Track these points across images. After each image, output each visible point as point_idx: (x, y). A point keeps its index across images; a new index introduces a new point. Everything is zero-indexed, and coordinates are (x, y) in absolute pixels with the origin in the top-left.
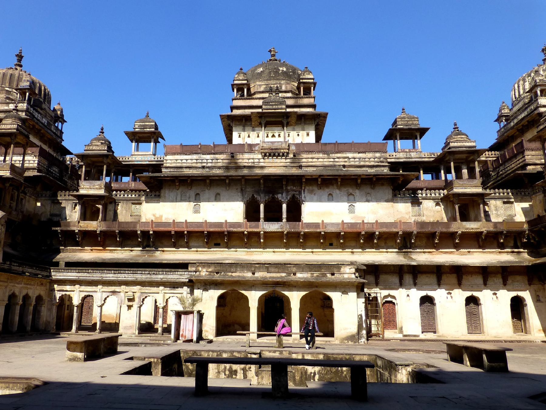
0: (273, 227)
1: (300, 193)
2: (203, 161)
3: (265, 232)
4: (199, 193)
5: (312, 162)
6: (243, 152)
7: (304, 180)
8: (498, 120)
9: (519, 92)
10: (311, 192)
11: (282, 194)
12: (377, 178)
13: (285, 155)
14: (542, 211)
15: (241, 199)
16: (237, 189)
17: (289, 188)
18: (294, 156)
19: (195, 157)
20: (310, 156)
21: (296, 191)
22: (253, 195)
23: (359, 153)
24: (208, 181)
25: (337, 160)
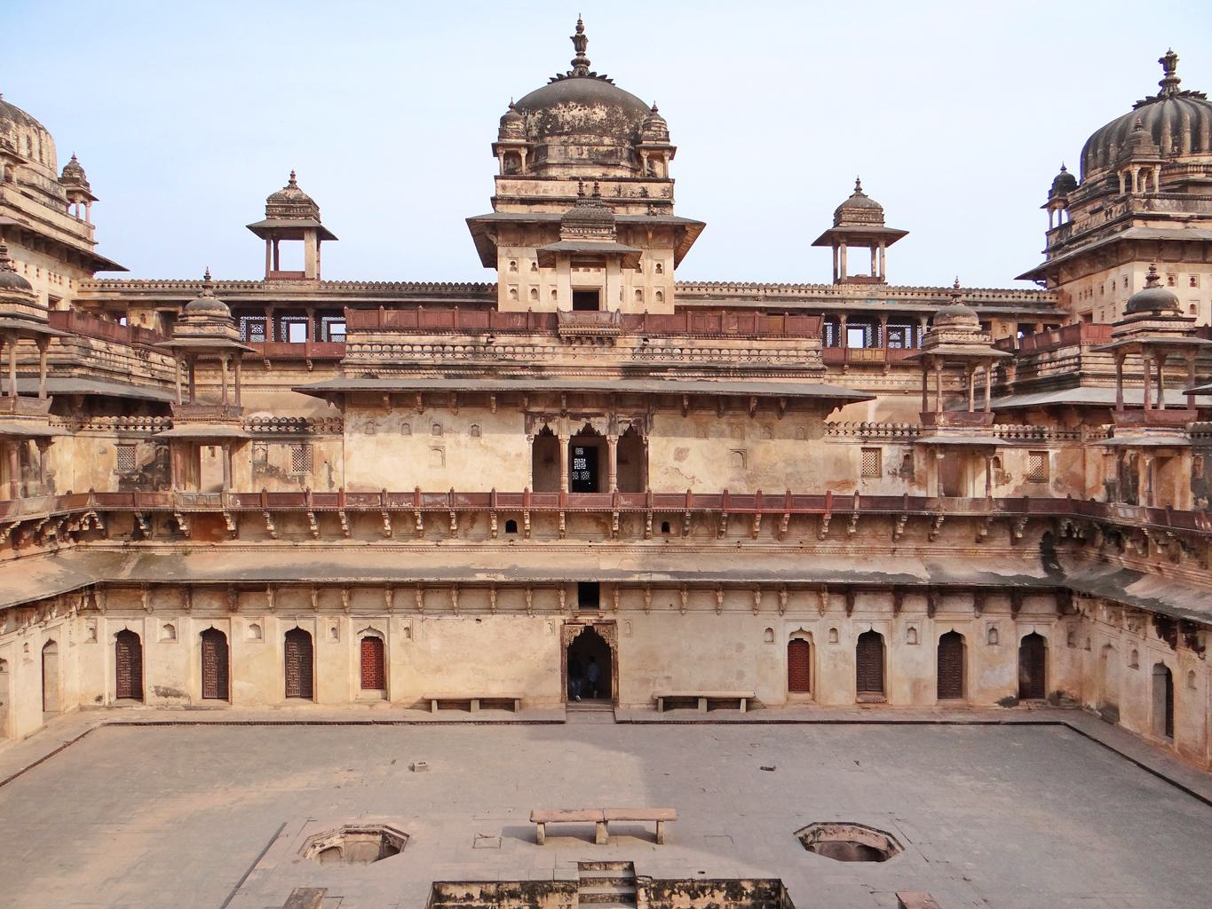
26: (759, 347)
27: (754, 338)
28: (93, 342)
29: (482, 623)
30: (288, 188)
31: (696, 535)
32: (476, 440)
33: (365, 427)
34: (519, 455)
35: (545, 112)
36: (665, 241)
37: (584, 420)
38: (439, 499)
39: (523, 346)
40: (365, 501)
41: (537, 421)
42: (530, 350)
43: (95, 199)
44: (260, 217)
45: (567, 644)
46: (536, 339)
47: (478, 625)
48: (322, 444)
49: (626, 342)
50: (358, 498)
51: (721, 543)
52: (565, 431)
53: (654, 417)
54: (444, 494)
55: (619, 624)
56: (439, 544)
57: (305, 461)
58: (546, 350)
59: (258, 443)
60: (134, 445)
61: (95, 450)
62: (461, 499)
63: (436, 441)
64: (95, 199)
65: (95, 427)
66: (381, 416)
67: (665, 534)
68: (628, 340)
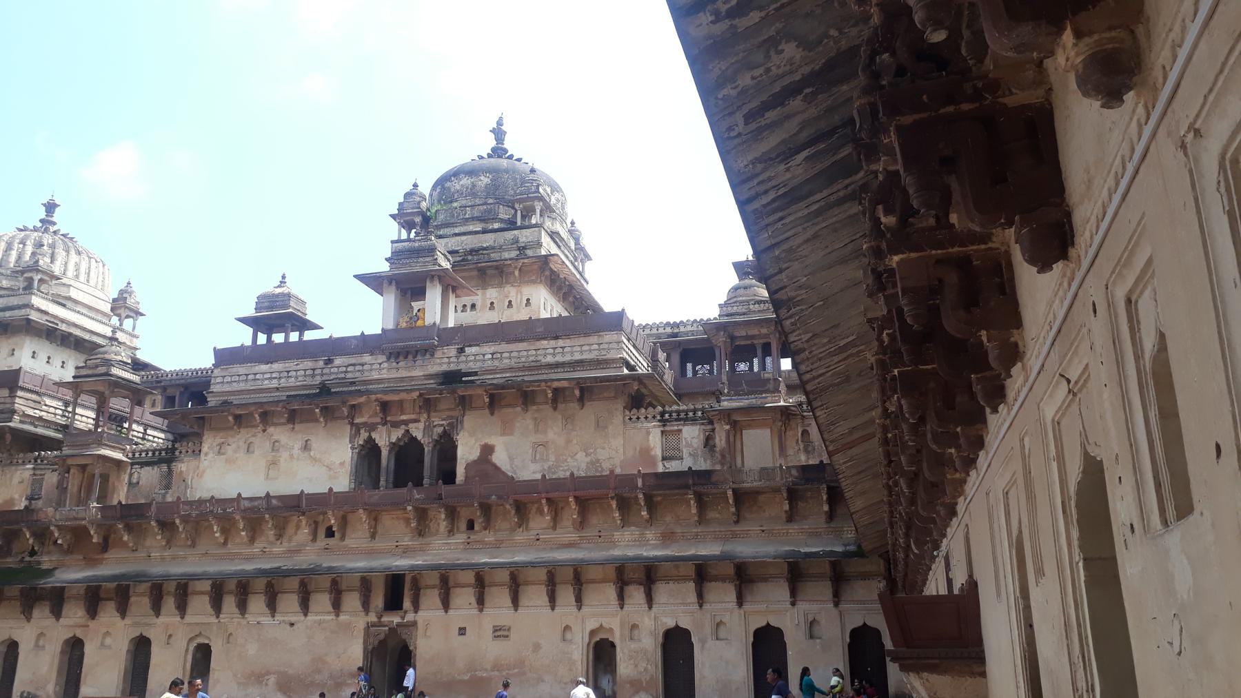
14: (21, 497)
26: (563, 345)
27: (556, 338)
28: (48, 401)
29: (295, 627)
31: (499, 530)
32: (306, 454)
33: (218, 447)
34: (342, 464)
35: (443, 187)
37: (403, 426)
38: (256, 503)
39: (354, 365)
40: (197, 509)
41: (362, 431)
42: (358, 368)
43: (142, 315)
44: (250, 311)
45: (370, 647)
46: (367, 358)
50: (192, 505)
52: (384, 439)
53: (465, 418)
54: (261, 498)
56: (265, 550)
57: (167, 481)
59: (135, 466)
60: (44, 474)
61: (16, 480)
62: (274, 502)
63: (273, 456)
64: (142, 315)
65: (20, 461)
66: (233, 436)
67: (469, 531)
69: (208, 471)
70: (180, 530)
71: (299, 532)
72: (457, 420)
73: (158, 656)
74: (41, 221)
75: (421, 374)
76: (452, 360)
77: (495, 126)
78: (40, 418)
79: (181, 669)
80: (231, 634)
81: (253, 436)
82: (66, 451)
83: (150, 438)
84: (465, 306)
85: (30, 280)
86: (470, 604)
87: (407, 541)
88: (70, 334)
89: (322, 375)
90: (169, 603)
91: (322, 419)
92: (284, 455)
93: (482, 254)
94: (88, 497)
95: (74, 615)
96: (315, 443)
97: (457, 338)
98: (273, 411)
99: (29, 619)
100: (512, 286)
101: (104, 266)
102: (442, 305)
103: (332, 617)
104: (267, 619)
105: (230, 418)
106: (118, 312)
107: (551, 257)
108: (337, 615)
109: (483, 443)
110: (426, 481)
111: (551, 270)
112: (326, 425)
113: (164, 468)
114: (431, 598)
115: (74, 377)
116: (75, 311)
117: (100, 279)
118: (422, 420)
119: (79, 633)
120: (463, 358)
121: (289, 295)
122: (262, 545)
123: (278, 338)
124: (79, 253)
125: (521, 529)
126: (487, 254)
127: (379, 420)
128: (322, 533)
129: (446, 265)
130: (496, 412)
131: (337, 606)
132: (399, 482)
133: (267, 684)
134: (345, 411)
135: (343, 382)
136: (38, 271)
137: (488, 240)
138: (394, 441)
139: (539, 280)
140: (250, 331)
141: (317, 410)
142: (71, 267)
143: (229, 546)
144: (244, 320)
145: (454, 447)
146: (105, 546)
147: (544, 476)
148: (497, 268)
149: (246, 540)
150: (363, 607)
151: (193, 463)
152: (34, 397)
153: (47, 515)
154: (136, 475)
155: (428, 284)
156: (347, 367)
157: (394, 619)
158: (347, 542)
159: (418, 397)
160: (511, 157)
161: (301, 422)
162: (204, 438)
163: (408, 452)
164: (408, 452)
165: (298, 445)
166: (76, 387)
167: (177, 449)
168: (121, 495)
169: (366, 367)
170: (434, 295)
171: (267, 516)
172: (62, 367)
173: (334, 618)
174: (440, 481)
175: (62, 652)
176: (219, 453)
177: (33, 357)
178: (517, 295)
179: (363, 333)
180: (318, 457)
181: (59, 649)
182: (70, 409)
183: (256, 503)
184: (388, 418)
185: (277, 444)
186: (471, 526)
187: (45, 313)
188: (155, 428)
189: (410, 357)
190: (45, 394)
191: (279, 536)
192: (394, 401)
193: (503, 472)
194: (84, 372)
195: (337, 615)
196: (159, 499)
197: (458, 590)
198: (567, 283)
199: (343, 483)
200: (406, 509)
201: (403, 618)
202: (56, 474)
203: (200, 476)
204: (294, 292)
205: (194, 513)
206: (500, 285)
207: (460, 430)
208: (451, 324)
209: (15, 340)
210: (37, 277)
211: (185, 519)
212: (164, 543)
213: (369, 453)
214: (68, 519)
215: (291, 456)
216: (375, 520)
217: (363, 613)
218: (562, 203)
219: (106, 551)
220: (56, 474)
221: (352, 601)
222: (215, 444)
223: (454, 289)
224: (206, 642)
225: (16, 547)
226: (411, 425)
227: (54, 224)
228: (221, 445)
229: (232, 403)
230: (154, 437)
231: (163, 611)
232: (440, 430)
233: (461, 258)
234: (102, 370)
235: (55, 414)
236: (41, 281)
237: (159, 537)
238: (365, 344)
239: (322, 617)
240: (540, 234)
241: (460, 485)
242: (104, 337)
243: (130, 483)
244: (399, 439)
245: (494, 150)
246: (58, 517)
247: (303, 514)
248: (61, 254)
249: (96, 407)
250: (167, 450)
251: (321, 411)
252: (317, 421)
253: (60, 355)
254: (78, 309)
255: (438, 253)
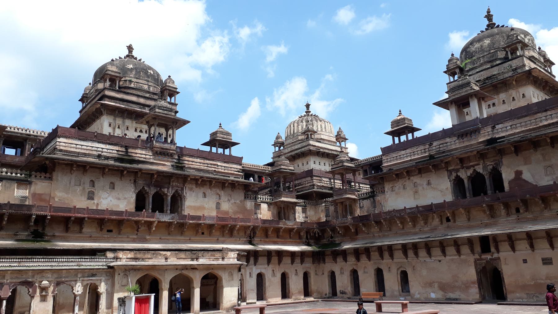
0: (166, 218)
1: (182, 189)
2: (99, 149)
3: (159, 222)
4: (94, 180)
5: (192, 165)
6: (136, 148)
7: (189, 179)
8: (275, 145)
9: (294, 129)
10: (191, 189)
11: (168, 189)
12: (238, 184)
13: (171, 155)
15: (134, 189)
16: (130, 180)
17: (174, 184)
18: (179, 157)
19: (90, 144)
20: (191, 159)
21: (179, 187)
22: (143, 186)
23: (225, 162)
24: (107, 170)
25: (209, 166)
26: (550, 114)
27: (546, 111)
28: (324, 179)
30: (399, 116)
32: (430, 186)
34: (447, 189)
35: (466, 52)
36: (524, 82)
37: (472, 168)
38: (413, 210)
39: (443, 144)
41: (453, 173)
42: (445, 145)
43: (347, 139)
44: (389, 129)
45: (479, 270)
46: (448, 140)
47: (441, 262)
48: (379, 197)
49: (485, 130)
51: (547, 214)
52: (464, 175)
53: (503, 159)
55: (501, 259)
58: (452, 143)
62: (421, 209)
63: (415, 189)
64: (347, 139)
65: (320, 203)
66: (397, 183)
68: (486, 129)
69: (389, 199)
70: (384, 224)
71: (434, 221)
72: (499, 162)
73: (386, 275)
74: (306, 112)
75: (475, 142)
76: (490, 133)
77: (486, 14)
78: (323, 186)
79: (397, 281)
80: (414, 266)
81: (405, 182)
82: (335, 198)
83: (361, 188)
84: (489, 105)
85: (308, 135)
86: (526, 248)
87: (486, 221)
88: (324, 152)
89: (429, 151)
90: (386, 255)
91: (433, 170)
92: (420, 188)
93: (493, 78)
94: (347, 215)
95: (352, 260)
96: (432, 182)
97: (490, 122)
98: (411, 170)
99: (336, 262)
100: (513, 89)
101: (330, 123)
102: (479, 107)
103: (457, 257)
104: (428, 259)
105: (394, 176)
106: (338, 140)
107: (532, 70)
108: (460, 256)
109: (516, 170)
110: (489, 192)
111: (533, 76)
112: (435, 171)
113: (372, 199)
114: (505, 246)
115: (332, 169)
116: (324, 143)
117: (330, 129)
118: (481, 164)
119: (355, 268)
120: (495, 131)
121: (404, 119)
122: (419, 228)
123: (403, 138)
124: (321, 121)
125: (547, 210)
126: (496, 77)
127: (460, 167)
128: (444, 221)
129: (477, 88)
130: (519, 154)
131: (459, 252)
132: (476, 193)
133: (434, 287)
134: (443, 165)
135: (439, 153)
136: (309, 131)
137: (495, 71)
138: (469, 175)
139: (528, 83)
140: (391, 137)
141: (431, 167)
142: (319, 127)
143: (405, 229)
144: (387, 133)
145: (501, 175)
146: (357, 233)
147: (555, 182)
148: (502, 83)
149: (411, 226)
150: (471, 251)
151: (383, 196)
152: (319, 178)
153: (333, 222)
154: (362, 204)
155: (470, 100)
156: (439, 145)
157: (489, 257)
158: (457, 223)
159: (477, 153)
160: (498, 26)
161: (425, 173)
162: (385, 185)
163: (477, 179)
164: (477, 179)
165: (425, 183)
166: (332, 172)
167: (375, 191)
168: (358, 213)
169: (448, 144)
170: (474, 104)
171: (419, 215)
172: (324, 165)
173: (458, 257)
174: (497, 191)
175: (350, 275)
176: (392, 190)
177: (314, 163)
178: (516, 93)
179: (443, 129)
180: (435, 187)
181: (349, 274)
182: (332, 181)
183: (413, 210)
184: (464, 165)
185: (416, 184)
186: (518, 211)
187: (315, 146)
188: (362, 184)
189: (468, 135)
190: (322, 177)
191: (426, 223)
192: (465, 157)
193: (530, 183)
194: (335, 166)
195: (460, 256)
196: (373, 212)
197: (518, 242)
198: (544, 80)
199: (449, 198)
200: (483, 206)
201: (492, 256)
202: (333, 206)
203: (386, 201)
204: (406, 117)
205: (388, 217)
206: (506, 91)
207: (502, 165)
208: (485, 116)
209: (307, 158)
210: (309, 134)
211: (385, 220)
212: (379, 230)
213: (458, 184)
214: (342, 223)
215: (423, 188)
216: (468, 211)
217: (472, 255)
218: (532, 40)
219: (357, 235)
220: (333, 206)
221: (465, 249)
222: (390, 187)
223: (483, 99)
224: (405, 270)
225: (326, 235)
226: (476, 167)
227: (310, 112)
228: (392, 187)
229: (393, 169)
230: (363, 187)
231: (385, 257)
232: (491, 167)
233: (483, 83)
234: (340, 165)
235: (327, 184)
236: (311, 134)
237: (376, 228)
238: (445, 133)
239: (453, 257)
240: (523, 59)
241: (507, 192)
242: (338, 151)
243: (360, 207)
244: (471, 174)
245: (488, 26)
246: (338, 223)
247: (435, 213)
248: (314, 122)
249: (341, 179)
250: (371, 192)
251: (432, 167)
252: (431, 171)
253: (323, 161)
254: (325, 142)
255: (472, 84)
